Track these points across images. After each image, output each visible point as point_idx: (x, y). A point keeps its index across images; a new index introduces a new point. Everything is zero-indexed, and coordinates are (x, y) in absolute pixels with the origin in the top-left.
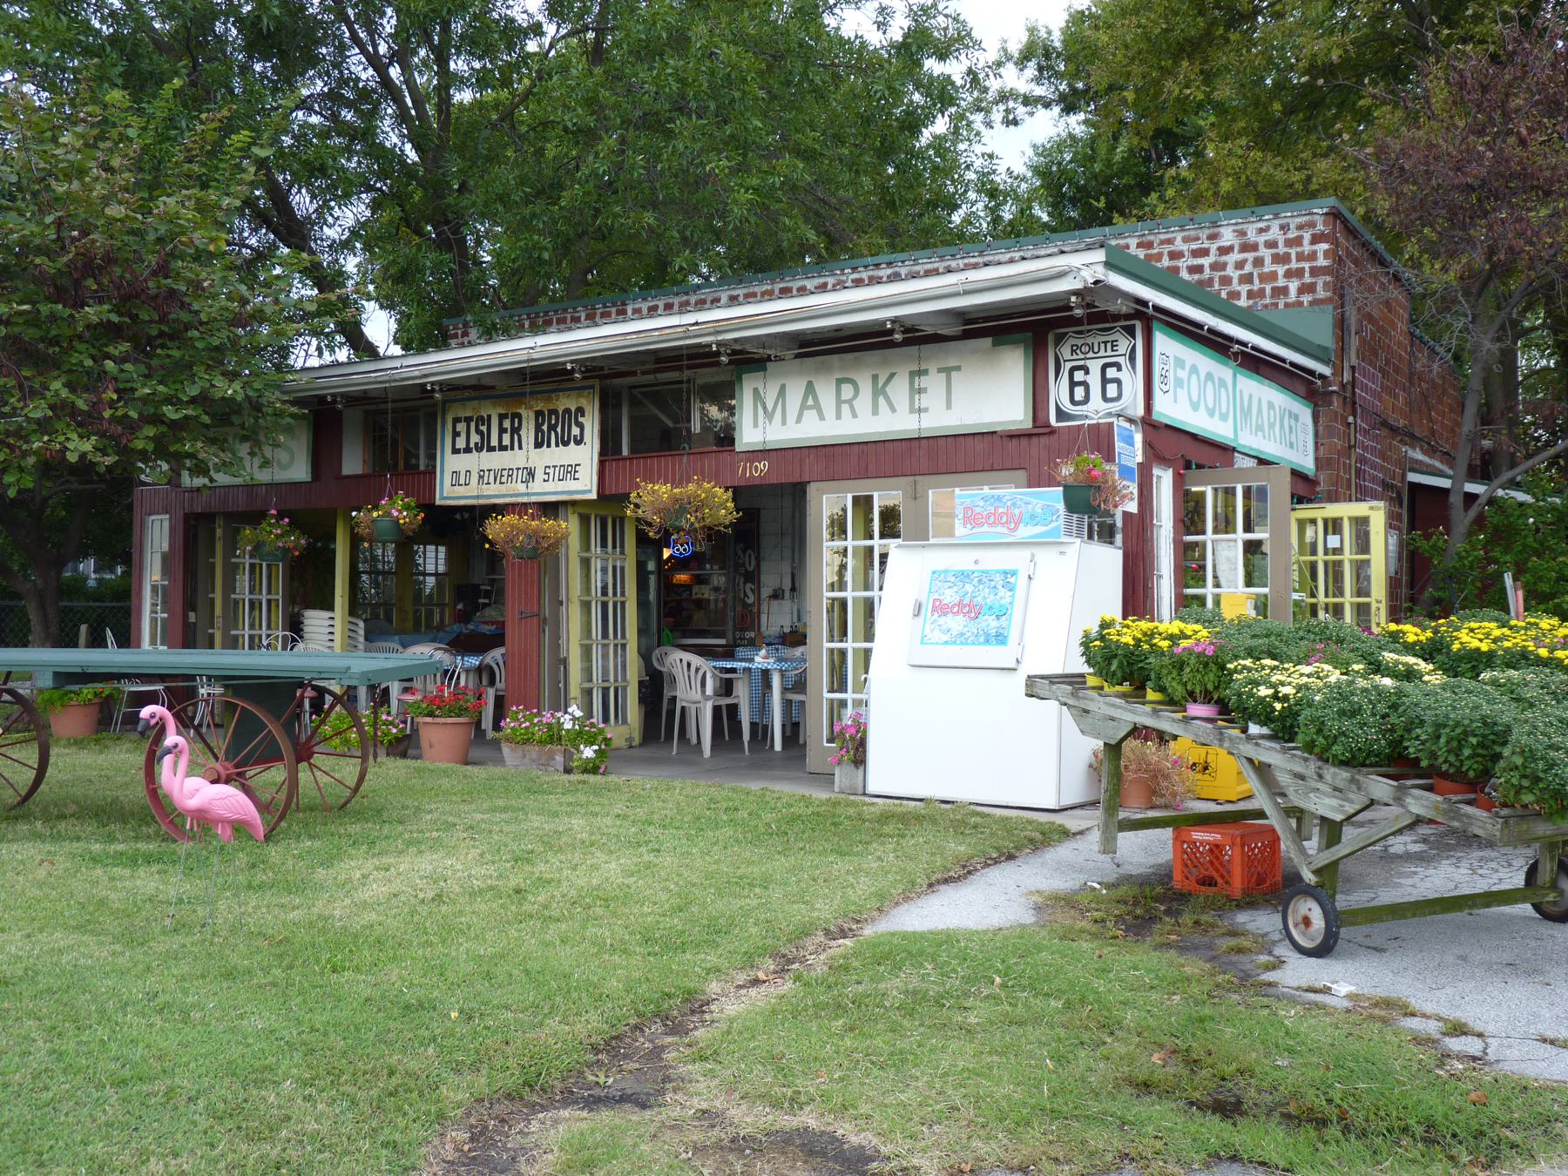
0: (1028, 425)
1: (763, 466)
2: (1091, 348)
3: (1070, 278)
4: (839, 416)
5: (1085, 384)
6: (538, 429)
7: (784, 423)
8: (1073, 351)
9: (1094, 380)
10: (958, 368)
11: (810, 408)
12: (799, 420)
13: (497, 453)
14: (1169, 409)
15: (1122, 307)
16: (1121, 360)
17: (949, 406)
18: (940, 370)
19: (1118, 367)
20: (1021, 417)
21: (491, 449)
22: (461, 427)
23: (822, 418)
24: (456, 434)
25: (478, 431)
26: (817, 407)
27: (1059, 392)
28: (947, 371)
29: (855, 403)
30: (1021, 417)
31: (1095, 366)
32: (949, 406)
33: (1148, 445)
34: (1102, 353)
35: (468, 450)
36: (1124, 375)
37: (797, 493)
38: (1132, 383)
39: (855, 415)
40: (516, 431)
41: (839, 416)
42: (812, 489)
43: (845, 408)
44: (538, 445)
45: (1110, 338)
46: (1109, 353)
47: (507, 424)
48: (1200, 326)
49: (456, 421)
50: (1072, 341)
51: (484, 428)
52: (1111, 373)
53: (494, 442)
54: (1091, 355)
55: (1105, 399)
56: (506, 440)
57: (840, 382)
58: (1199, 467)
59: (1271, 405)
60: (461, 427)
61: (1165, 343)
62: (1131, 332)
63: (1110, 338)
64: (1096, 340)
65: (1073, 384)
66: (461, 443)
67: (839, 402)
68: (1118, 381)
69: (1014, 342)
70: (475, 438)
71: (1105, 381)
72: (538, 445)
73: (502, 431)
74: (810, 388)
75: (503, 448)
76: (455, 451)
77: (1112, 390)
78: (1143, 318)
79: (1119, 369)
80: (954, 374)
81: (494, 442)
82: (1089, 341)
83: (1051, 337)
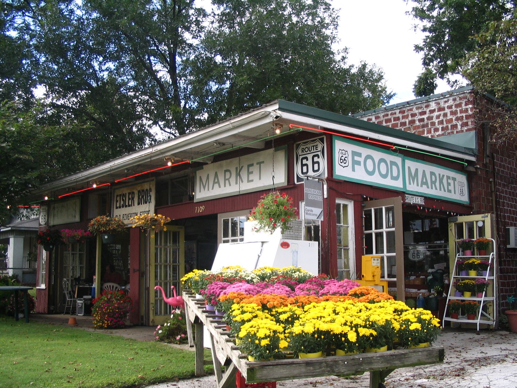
0: (286, 184)
1: (202, 208)
2: (309, 149)
3: (269, 117)
4: (225, 186)
5: (307, 165)
6: (139, 198)
7: (208, 190)
8: (302, 151)
9: (310, 163)
10: (263, 162)
11: (216, 183)
12: (213, 189)
13: (128, 208)
14: (342, 172)
15: (319, 131)
16: (319, 153)
17: (260, 179)
18: (257, 164)
19: (318, 156)
20: (283, 181)
21: (126, 206)
22: (118, 198)
23: (220, 187)
24: (117, 201)
25: (123, 200)
26: (218, 183)
27: (298, 170)
28: (259, 163)
29: (230, 180)
30: (283, 181)
31: (310, 157)
32: (260, 179)
33: (329, 189)
34: (312, 151)
35: (120, 207)
36: (320, 160)
37: (214, 218)
38: (323, 163)
39: (230, 185)
40: (133, 199)
41: (225, 186)
42: (219, 215)
43: (227, 182)
44: (139, 204)
45: (315, 144)
46: (315, 151)
47: (130, 197)
48: (366, 138)
49: (117, 196)
50: (302, 147)
51: (124, 198)
52: (316, 159)
53: (127, 204)
54: (309, 152)
55: (314, 171)
56: (130, 203)
57: (226, 171)
58: (371, 199)
59: (432, 174)
60: (118, 198)
61: (339, 145)
62: (322, 140)
63: (315, 144)
64: (310, 145)
65: (303, 165)
66: (118, 205)
67: (225, 180)
68: (318, 163)
69: (281, 149)
70: (122, 203)
71: (314, 163)
72: (139, 204)
73: (129, 199)
74: (216, 175)
75: (129, 206)
76: (117, 208)
77: (316, 166)
78: (329, 136)
79: (319, 157)
80: (262, 165)
81: (127, 204)
82: (308, 146)
83: (295, 145)
